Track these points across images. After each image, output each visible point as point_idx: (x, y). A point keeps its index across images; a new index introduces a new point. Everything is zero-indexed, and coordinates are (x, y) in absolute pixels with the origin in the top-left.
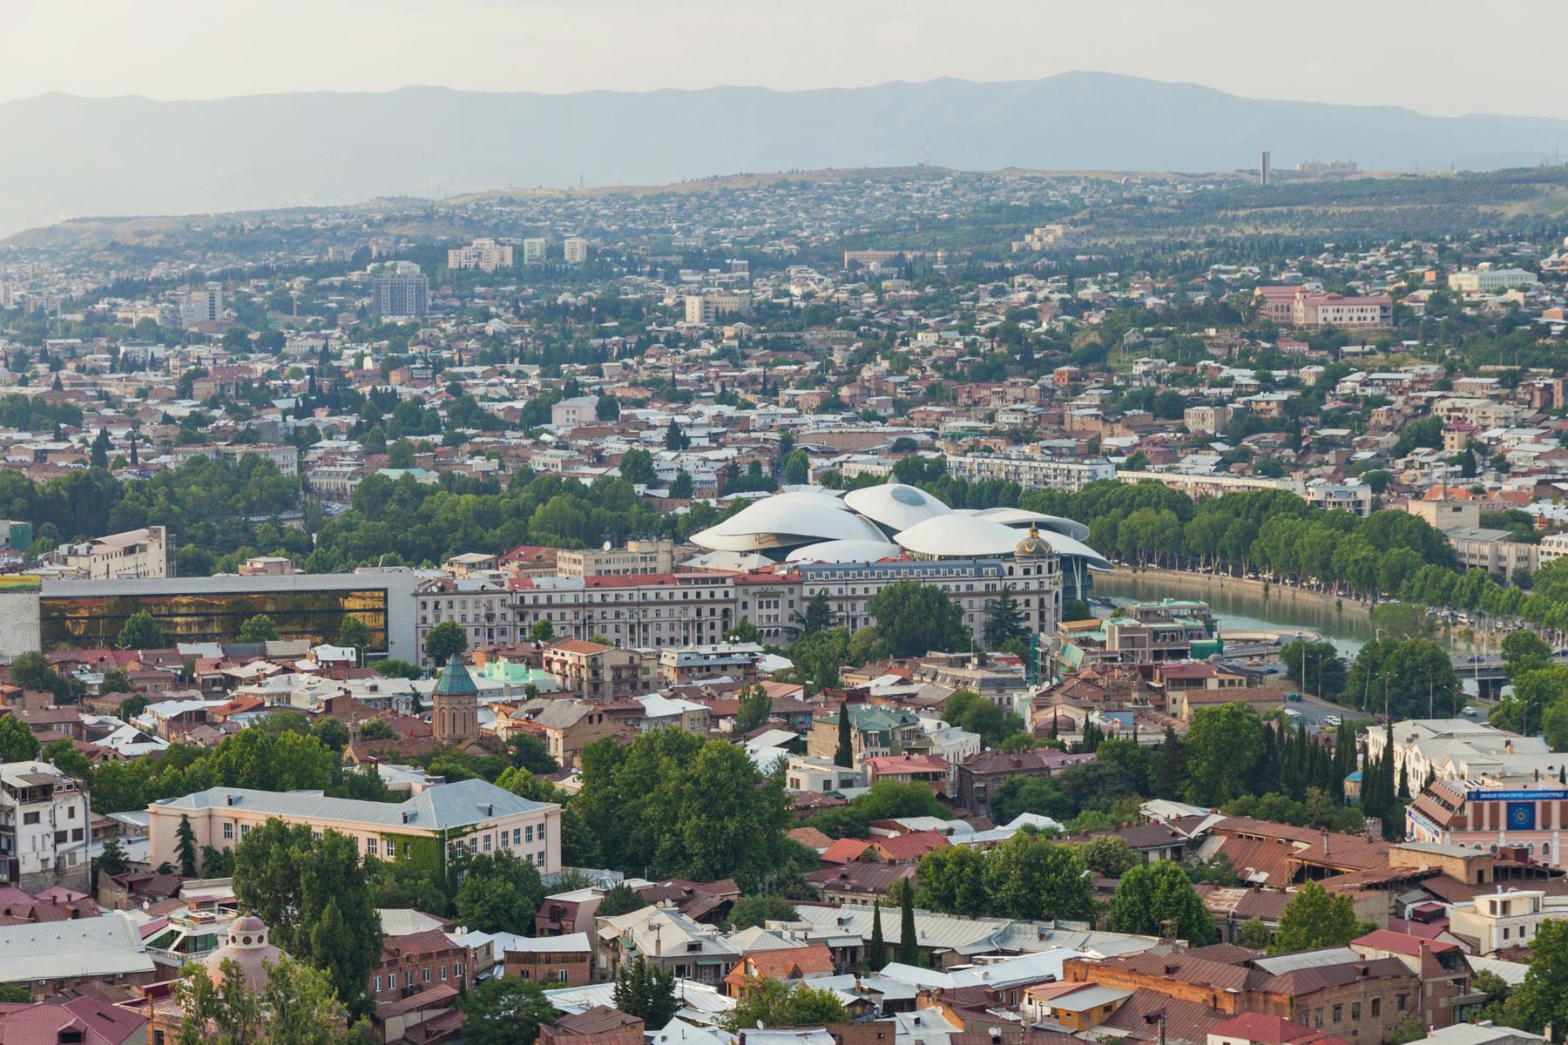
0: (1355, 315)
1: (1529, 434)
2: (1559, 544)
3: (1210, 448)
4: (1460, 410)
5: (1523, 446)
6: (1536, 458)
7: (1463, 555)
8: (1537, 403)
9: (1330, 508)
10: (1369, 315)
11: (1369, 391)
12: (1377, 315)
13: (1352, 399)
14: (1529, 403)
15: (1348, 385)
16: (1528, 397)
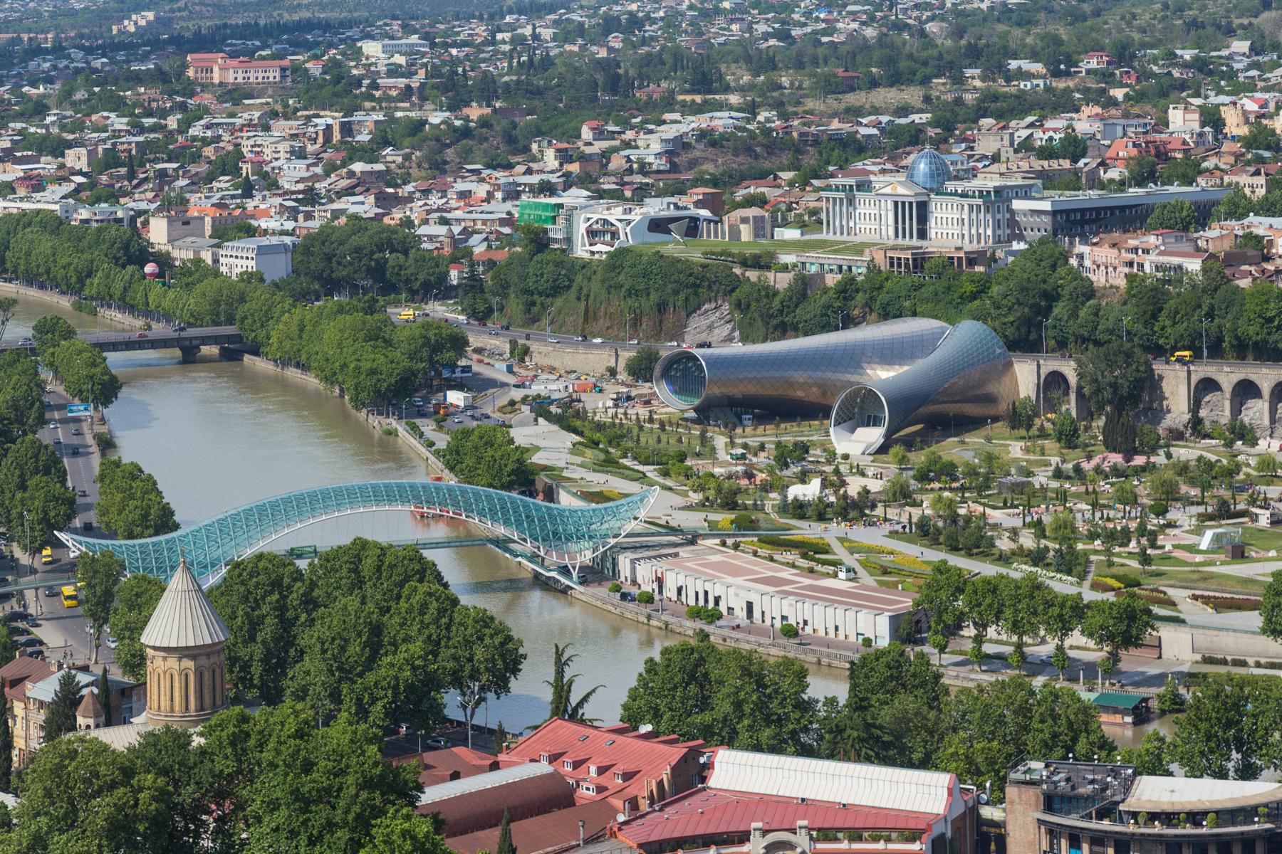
0: (260, 75)
1: (301, 164)
2: (232, 248)
3: (71, 181)
4: (259, 146)
5: (292, 174)
6: (297, 182)
7: (174, 259)
8: (320, 140)
9: (95, 225)
10: (271, 75)
11: (209, 133)
12: (277, 74)
13: (194, 139)
14: (315, 140)
15: (196, 130)
16: (314, 136)
